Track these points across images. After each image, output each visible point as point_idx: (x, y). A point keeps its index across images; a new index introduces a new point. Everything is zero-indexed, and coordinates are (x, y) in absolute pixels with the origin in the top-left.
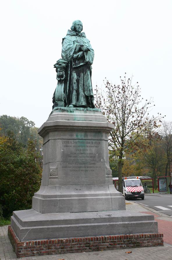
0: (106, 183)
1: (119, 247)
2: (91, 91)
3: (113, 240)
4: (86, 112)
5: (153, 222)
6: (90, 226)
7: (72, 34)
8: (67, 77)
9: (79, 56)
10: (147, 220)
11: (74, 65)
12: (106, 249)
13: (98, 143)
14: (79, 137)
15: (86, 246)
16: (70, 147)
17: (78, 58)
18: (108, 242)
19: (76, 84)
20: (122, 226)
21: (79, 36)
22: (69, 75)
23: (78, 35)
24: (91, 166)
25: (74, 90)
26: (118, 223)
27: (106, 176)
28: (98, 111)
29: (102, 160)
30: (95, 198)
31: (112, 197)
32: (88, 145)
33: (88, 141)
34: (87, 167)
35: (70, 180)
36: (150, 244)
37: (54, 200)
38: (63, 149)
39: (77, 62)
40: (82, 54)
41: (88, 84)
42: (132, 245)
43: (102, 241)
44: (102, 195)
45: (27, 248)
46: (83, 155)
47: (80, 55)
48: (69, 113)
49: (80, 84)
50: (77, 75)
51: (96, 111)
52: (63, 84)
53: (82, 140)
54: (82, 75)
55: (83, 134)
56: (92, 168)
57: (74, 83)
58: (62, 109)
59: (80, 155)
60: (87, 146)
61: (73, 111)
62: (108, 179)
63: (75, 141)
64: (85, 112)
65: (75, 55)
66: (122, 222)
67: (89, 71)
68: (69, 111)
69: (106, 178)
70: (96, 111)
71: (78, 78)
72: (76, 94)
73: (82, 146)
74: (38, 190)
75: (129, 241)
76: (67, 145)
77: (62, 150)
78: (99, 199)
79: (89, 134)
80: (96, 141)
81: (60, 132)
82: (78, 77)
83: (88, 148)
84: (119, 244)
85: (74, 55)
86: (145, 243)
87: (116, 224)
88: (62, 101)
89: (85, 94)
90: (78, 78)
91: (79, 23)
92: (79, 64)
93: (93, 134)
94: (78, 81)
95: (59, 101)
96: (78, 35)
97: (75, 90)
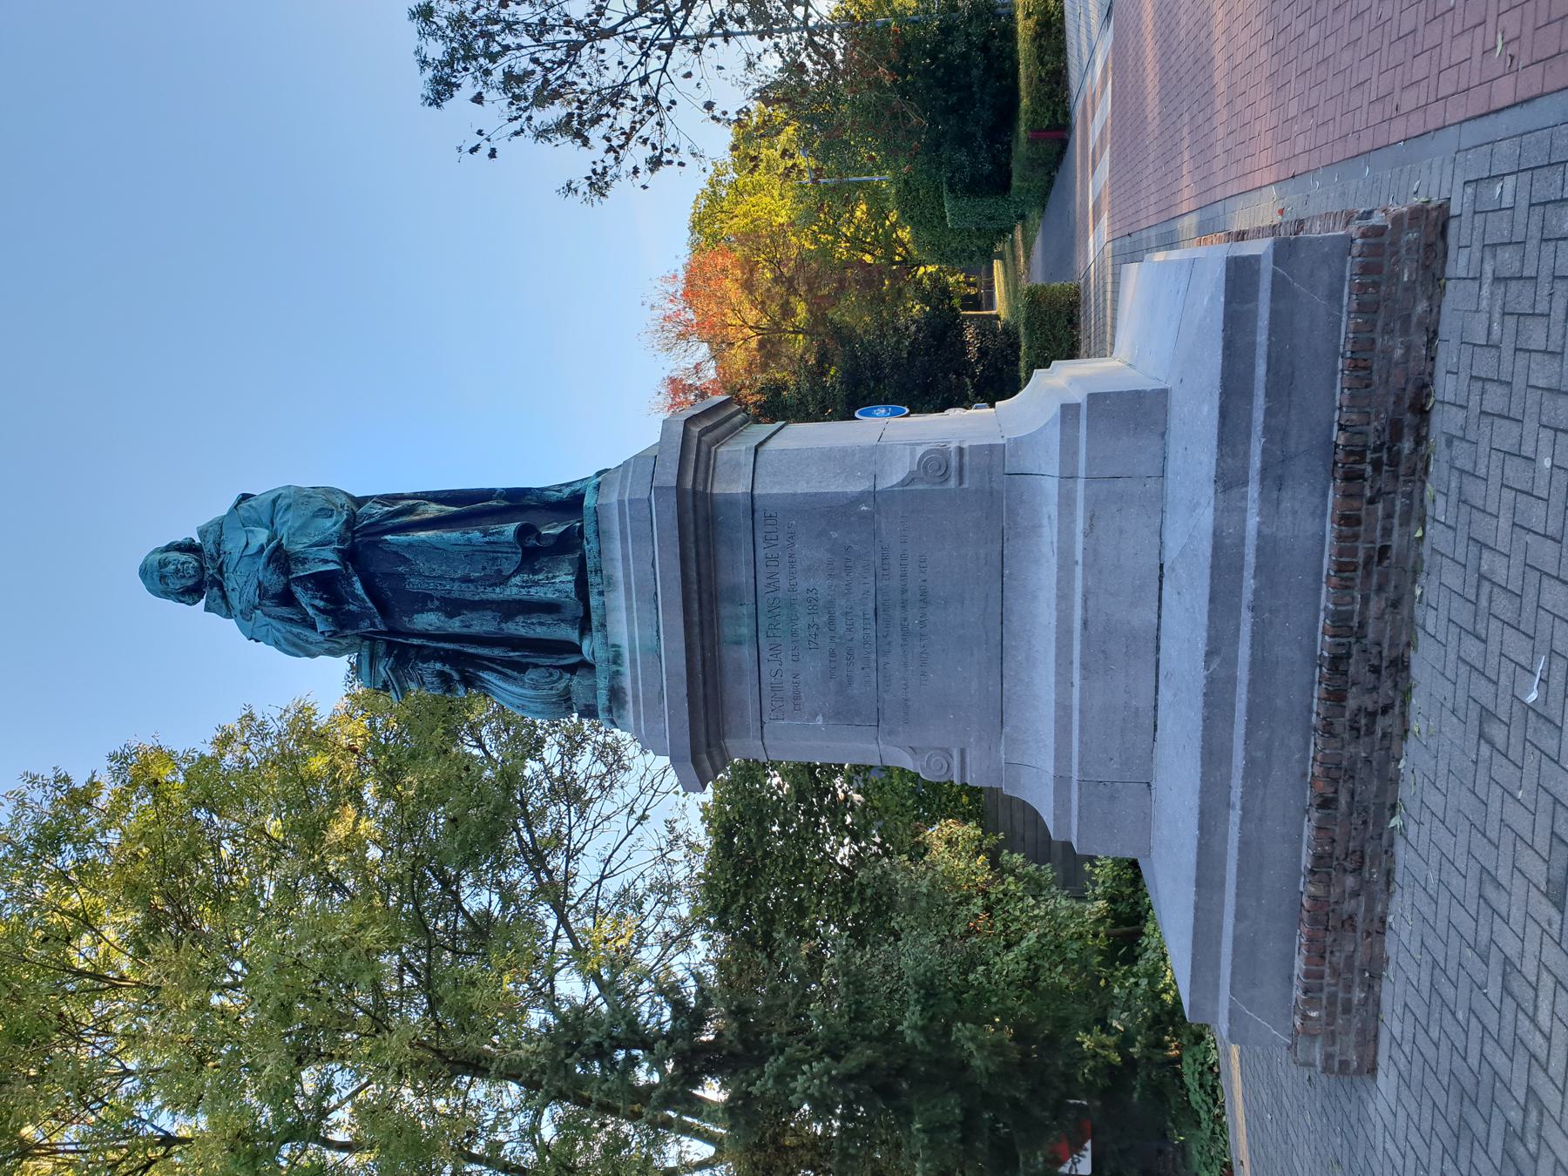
0: (995, 485)
2: (492, 539)
3: (1355, 570)
4: (610, 578)
5: (1275, 273)
6: (1252, 685)
8: (445, 657)
9: (321, 604)
10: (1254, 315)
11: (373, 625)
12: (1405, 612)
13: (770, 528)
14: (745, 631)
16: (801, 677)
17: (330, 607)
18: (1366, 600)
19: (468, 616)
20: (1275, 495)
21: (222, 575)
23: (218, 577)
26: (1253, 522)
27: (953, 483)
29: (864, 508)
30: (1085, 578)
31: (1082, 473)
32: (784, 583)
33: (762, 581)
34: (904, 591)
36: (1422, 306)
40: (306, 589)
41: (456, 548)
42: (1407, 445)
44: (1066, 532)
47: (314, 597)
48: (626, 669)
49: (468, 596)
53: (762, 619)
54: (414, 584)
55: (726, 610)
57: (465, 630)
58: (610, 701)
59: (841, 628)
60: (792, 589)
61: (614, 646)
63: (765, 654)
64: (609, 584)
65: (320, 628)
66: (1246, 483)
67: (388, 537)
68: (614, 668)
69: (966, 485)
71: (437, 603)
72: (520, 619)
74: (1025, 805)
75: (1377, 464)
77: (820, 720)
78: (1092, 553)
79: (726, 578)
80: (759, 540)
81: (726, 727)
83: (803, 585)
84: (1387, 532)
85: (323, 633)
86: (1408, 348)
87: (1259, 533)
88: (567, 689)
89: (513, 574)
90: (437, 603)
91: (157, 579)
92: (363, 600)
93: (724, 553)
94: (452, 607)
95: (570, 699)
96: (218, 577)
97: (503, 625)
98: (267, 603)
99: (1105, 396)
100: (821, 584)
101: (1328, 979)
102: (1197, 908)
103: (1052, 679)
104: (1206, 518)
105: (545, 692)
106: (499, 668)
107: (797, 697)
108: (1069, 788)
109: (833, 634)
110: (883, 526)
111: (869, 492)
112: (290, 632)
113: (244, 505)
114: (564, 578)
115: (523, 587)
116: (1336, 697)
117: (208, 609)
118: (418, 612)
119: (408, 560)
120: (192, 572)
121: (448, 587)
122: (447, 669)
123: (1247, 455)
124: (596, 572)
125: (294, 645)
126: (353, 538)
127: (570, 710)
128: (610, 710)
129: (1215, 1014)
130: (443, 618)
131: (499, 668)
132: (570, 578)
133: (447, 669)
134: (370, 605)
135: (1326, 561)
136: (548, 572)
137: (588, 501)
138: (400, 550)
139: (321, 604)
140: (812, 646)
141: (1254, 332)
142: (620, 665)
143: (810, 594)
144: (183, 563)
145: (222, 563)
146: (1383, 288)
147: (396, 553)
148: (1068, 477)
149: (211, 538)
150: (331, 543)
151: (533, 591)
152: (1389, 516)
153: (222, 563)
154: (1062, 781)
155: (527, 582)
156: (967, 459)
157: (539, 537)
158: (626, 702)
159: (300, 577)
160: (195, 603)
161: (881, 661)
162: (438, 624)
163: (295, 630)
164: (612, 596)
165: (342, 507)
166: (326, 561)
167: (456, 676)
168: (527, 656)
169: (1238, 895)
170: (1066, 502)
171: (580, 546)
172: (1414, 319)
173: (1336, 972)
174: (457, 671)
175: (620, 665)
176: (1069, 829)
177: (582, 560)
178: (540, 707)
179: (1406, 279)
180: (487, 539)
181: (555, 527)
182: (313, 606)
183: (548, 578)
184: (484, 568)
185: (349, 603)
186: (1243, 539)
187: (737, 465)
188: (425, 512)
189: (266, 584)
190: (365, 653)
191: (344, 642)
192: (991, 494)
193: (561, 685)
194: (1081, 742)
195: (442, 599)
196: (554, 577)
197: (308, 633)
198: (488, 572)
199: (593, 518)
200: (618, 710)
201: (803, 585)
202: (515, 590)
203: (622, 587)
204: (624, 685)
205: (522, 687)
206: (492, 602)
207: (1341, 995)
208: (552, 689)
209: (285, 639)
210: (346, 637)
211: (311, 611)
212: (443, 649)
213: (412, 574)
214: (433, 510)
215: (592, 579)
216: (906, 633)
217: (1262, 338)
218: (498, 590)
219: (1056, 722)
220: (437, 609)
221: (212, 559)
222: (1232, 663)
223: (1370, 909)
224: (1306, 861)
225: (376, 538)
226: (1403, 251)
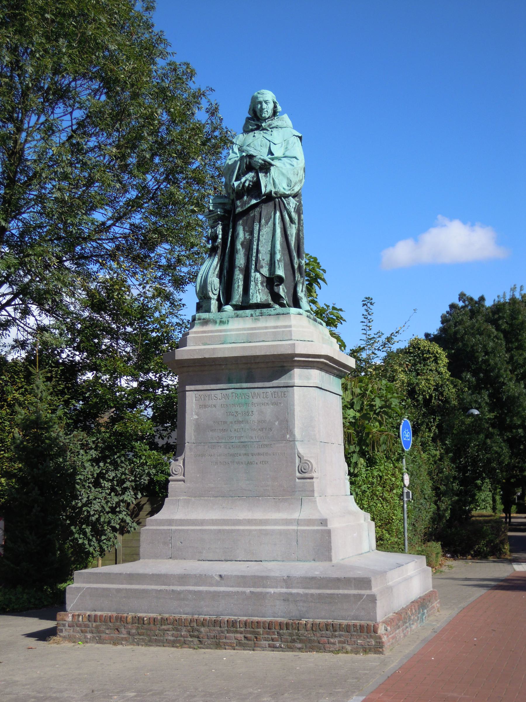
0: (297, 493)
1: (267, 646)
4: (258, 320)
5: (364, 595)
9: (247, 184)
15: (191, 636)
17: (245, 189)
18: (241, 633)
20: (282, 598)
24: (262, 450)
26: (272, 590)
27: (298, 474)
29: (288, 436)
30: (256, 530)
31: (299, 528)
32: (255, 400)
35: (212, 485)
37: (164, 530)
38: (197, 414)
42: (299, 645)
43: (226, 628)
44: (276, 522)
45: (73, 626)
46: (242, 425)
48: (217, 327)
51: (283, 314)
53: (240, 390)
56: (262, 457)
58: (204, 319)
59: (236, 427)
61: (228, 321)
62: (304, 483)
64: (256, 319)
68: (218, 321)
69: (297, 480)
70: (283, 314)
73: (240, 405)
76: (207, 404)
77: (196, 417)
78: (267, 533)
80: (274, 389)
83: (255, 409)
86: (334, 644)
87: (268, 593)
92: (249, 203)
95: (205, 298)
97: (238, 269)
99: (330, 536)
100: (255, 418)
101: (94, 624)
102: (120, 574)
103: (214, 518)
104: (276, 574)
107: (205, 406)
108: (169, 525)
109: (233, 422)
110: (281, 445)
111: (295, 439)
116: (203, 624)
123: (298, 588)
124: (261, 313)
129: (78, 582)
135: (256, 618)
136: (262, 290)
137: (293, 310)
140: (228, 413)
141: (343, 589)
142: (220, 324)
143: (251, 412)
145: (268, 130)
146: (355, 633)
148: (298, 522)
150: (275, 188)
152: (273, 640)
153: (268, 130)
154: (170, 522)
155: (257, 280)
156: (308, 480)
157: (278, 285)
161: (222, 444)
164: (250, 321)
165: (293, 190)
166: (266, 187)
169: (126, 589)
170: (288, 522)
172: (344, 645)
173: (97, 627)
175: (220, 324)
176: (152, 525)
177: (268, 306)
179: (358, 641)
181: (284, 291)
183: (259, 290)
184: (263, 260)
186: (266, 587)
187: (308, 378)
188: (291, 228)
190: (226, 201)
192: (293, 492)
194: (188, 530)
196: (259, 293)
201: (255, 409)
207: (89, 629)
214: (293, 231)
215: (258, 311)
216: (233, 455)
217: (341, 592)
219: (196, 520)
222: (218, 584)
223: (123, 639)
224: (140, 615)
226: (368, 640)
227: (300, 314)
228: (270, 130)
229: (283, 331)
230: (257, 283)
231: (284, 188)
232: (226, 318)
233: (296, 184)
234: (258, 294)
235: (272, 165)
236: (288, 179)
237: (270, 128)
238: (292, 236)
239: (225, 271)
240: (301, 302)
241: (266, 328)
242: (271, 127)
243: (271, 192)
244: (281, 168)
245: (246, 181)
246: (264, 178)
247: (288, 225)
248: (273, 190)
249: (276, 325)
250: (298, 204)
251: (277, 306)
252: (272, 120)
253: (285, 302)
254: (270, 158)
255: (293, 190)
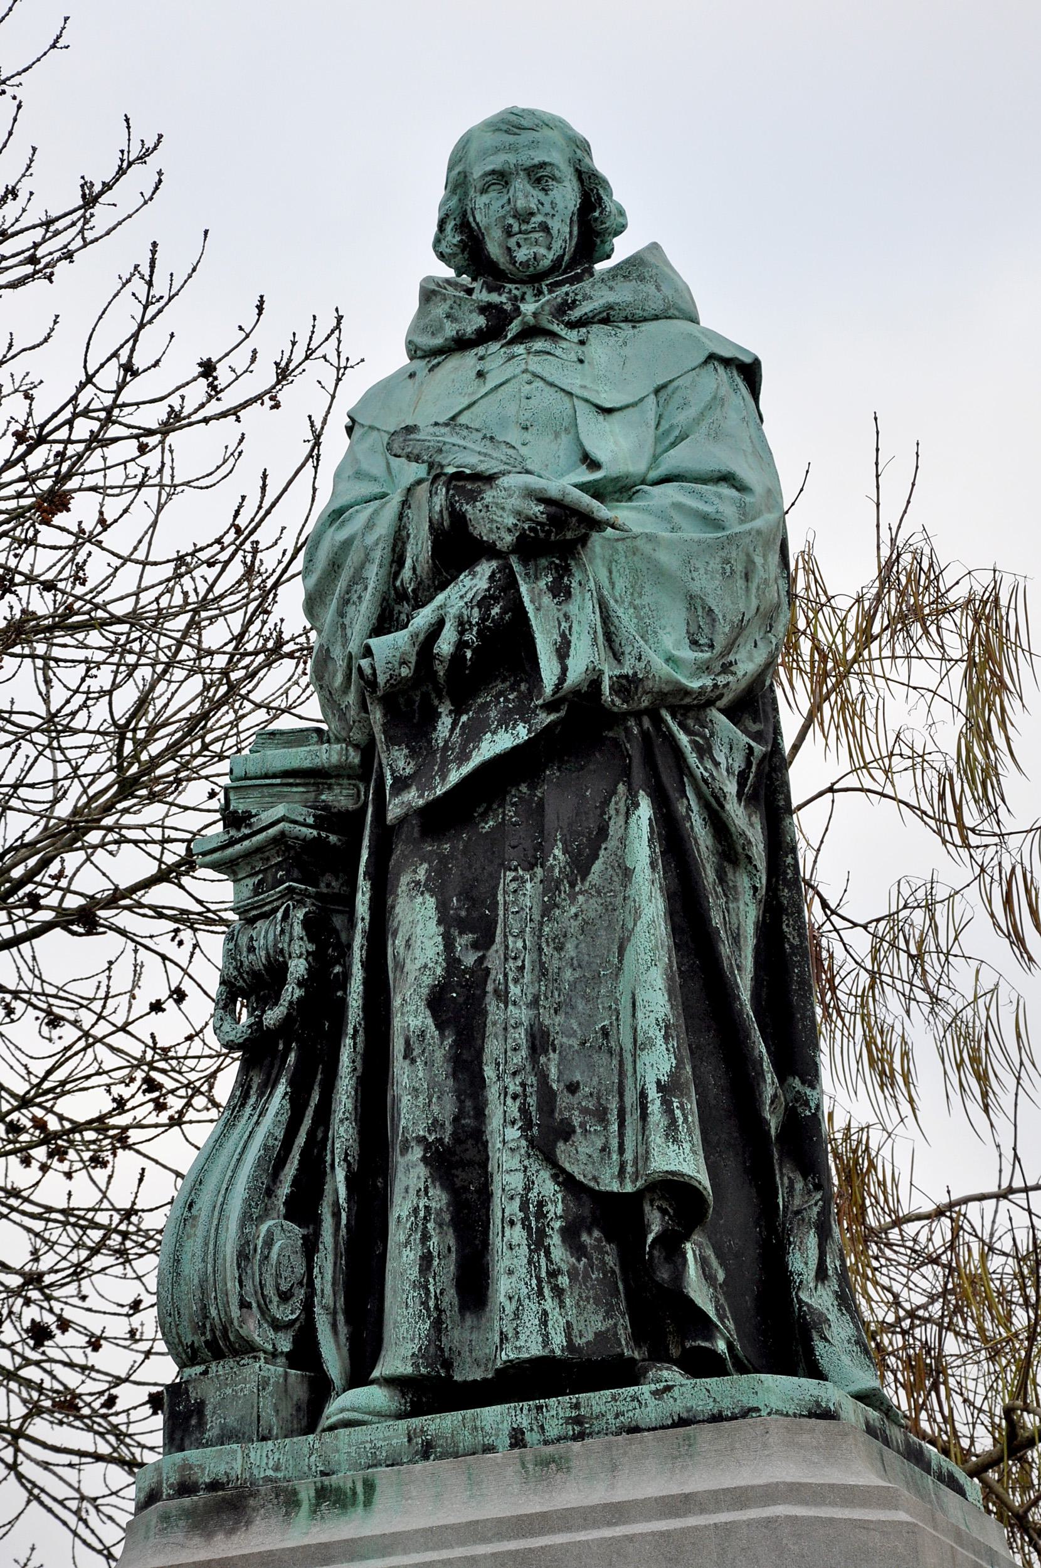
2: (655, 1107)
4: (559, 1463)
7: (438, 341)
9: (445, 645)
11: (402, 784)
17: (441, 670)
19: (439, 1047)
21: (521, 337)
22: (358, 941)
23: (514, 328)
25: (405, 1149)
28: (747, 1412)
39: (444, 724)
40: (484, 603)
47: (462, 625)
49: (493, 1048)
50: (443, 918)
51: (717, 1418)
52: (282, 1088)
57: (398, 1046)
61: (370, 1486)
64: (544, 1462)
67: (645, 810)
68: (306, 1493)
70: (717, 1418)
71: (469, 959)
72: (439, 1198)
82: (462, 941)
85: (368, 652)
88: (248, 1348)
90: (469, 959)
91: (496, 162)
92: (464, 757)
95: (218, 1355)
96: (514, 328)
97: (417, 1153)
98: (440, 501)
105: (232, 1286)
106: (301, 1140)
112: (367, 559)
113: (721, 380)
114: (557, 1321)
115: (524, 1207)
117: (429, 293)
118: (442, 907)
119: (585, 872)
120: (522, 255)
121: (514, 990)
122: (291, 992)
124: (578, 1421)
125: (335, 566)
126: (638, 715)
127: (186, 1356)
128: (185, 1488)
130: (427, 980)
131: (301, 1140)
132: (558, 1340)
133: (291, 992)
134: (454, 777)
136: (573, 1274)
138: (612, 843)
139: (445, 645)
142: (314, 1510)
144: (545, 228)
147: (603, 833)
149: (622, 294)
151: (517, 1234)
155: (541, 1215)
157: (672, 1244)
158: (209, 1535)
159: (513, 584)
160: (441, 256)
162: (412, 968)
163: (374, 574)
165: (726, 668)
166: (563, 651)
167: (273, 1016)
168: (336, 1215)
171: (659, 1355)
174: (288, 1019)
175: (314, 1510)
178: (191, 1269)
180: (653, 1093)
181: (708, 1276)
182: (440, 624)
183: (553, 1274)
184: (573, 1088)
185: (457, 712)
189: (489, 496)
190: (329, 755)
191: (351, 698)
193: (254, 1330)
195: (481, 973)
196: (558, 1292)
197: (363, 612)
198: (564, 1100)
199: (727, 1406)
200: (188, 1514)
202: (516, 1182)
203: (533, 1505)
204: (259, 1524)
205: (247, 1218)
206: (480, 1114)
208: (244, 1305)
209: (347, 544)
210: (364, 707)
211: (423, 618)
212: (347, 976)
213: (551, 886)
215: (558, 1407)
218: (513, 1133)
220: (452, 963)
221: (562, 309)
225: (638, 773)
227: (827, 1415)
228: (573, 335)
229: (728, 1529)
230: (542, 1234)
231: (670, 659)
232: (356, 1466)
233: (740, 628)
234: (549, 1304)
235: (595, 524)
236: (692, 601)
237: (571, 325)
238: (736, 939)
239: (340, 1174)
240: (819, 1346)
241: (617, 1512)
242: (575, 314)
243: (595, 684)
244: (650, 538)
245: (440, 624)
246: (547, 599)
247: (709, 875)
248: (609, 671)
249: (674, 1489)
250: (759, 749)
251: (671, 1375)
252: (578, 279)
253: (721, 1346)
254: (582, 487)
255: (726, 668)
